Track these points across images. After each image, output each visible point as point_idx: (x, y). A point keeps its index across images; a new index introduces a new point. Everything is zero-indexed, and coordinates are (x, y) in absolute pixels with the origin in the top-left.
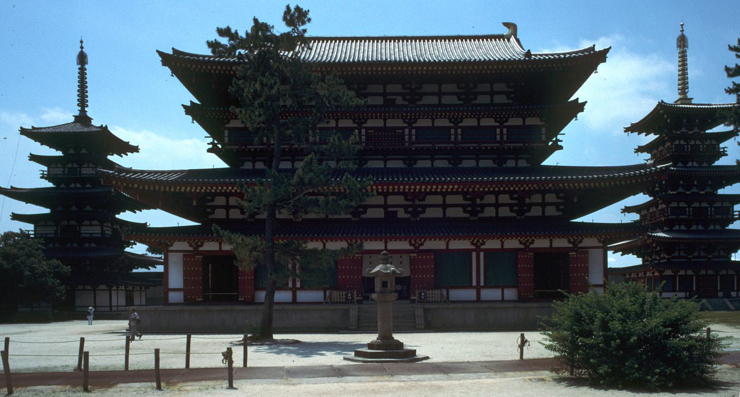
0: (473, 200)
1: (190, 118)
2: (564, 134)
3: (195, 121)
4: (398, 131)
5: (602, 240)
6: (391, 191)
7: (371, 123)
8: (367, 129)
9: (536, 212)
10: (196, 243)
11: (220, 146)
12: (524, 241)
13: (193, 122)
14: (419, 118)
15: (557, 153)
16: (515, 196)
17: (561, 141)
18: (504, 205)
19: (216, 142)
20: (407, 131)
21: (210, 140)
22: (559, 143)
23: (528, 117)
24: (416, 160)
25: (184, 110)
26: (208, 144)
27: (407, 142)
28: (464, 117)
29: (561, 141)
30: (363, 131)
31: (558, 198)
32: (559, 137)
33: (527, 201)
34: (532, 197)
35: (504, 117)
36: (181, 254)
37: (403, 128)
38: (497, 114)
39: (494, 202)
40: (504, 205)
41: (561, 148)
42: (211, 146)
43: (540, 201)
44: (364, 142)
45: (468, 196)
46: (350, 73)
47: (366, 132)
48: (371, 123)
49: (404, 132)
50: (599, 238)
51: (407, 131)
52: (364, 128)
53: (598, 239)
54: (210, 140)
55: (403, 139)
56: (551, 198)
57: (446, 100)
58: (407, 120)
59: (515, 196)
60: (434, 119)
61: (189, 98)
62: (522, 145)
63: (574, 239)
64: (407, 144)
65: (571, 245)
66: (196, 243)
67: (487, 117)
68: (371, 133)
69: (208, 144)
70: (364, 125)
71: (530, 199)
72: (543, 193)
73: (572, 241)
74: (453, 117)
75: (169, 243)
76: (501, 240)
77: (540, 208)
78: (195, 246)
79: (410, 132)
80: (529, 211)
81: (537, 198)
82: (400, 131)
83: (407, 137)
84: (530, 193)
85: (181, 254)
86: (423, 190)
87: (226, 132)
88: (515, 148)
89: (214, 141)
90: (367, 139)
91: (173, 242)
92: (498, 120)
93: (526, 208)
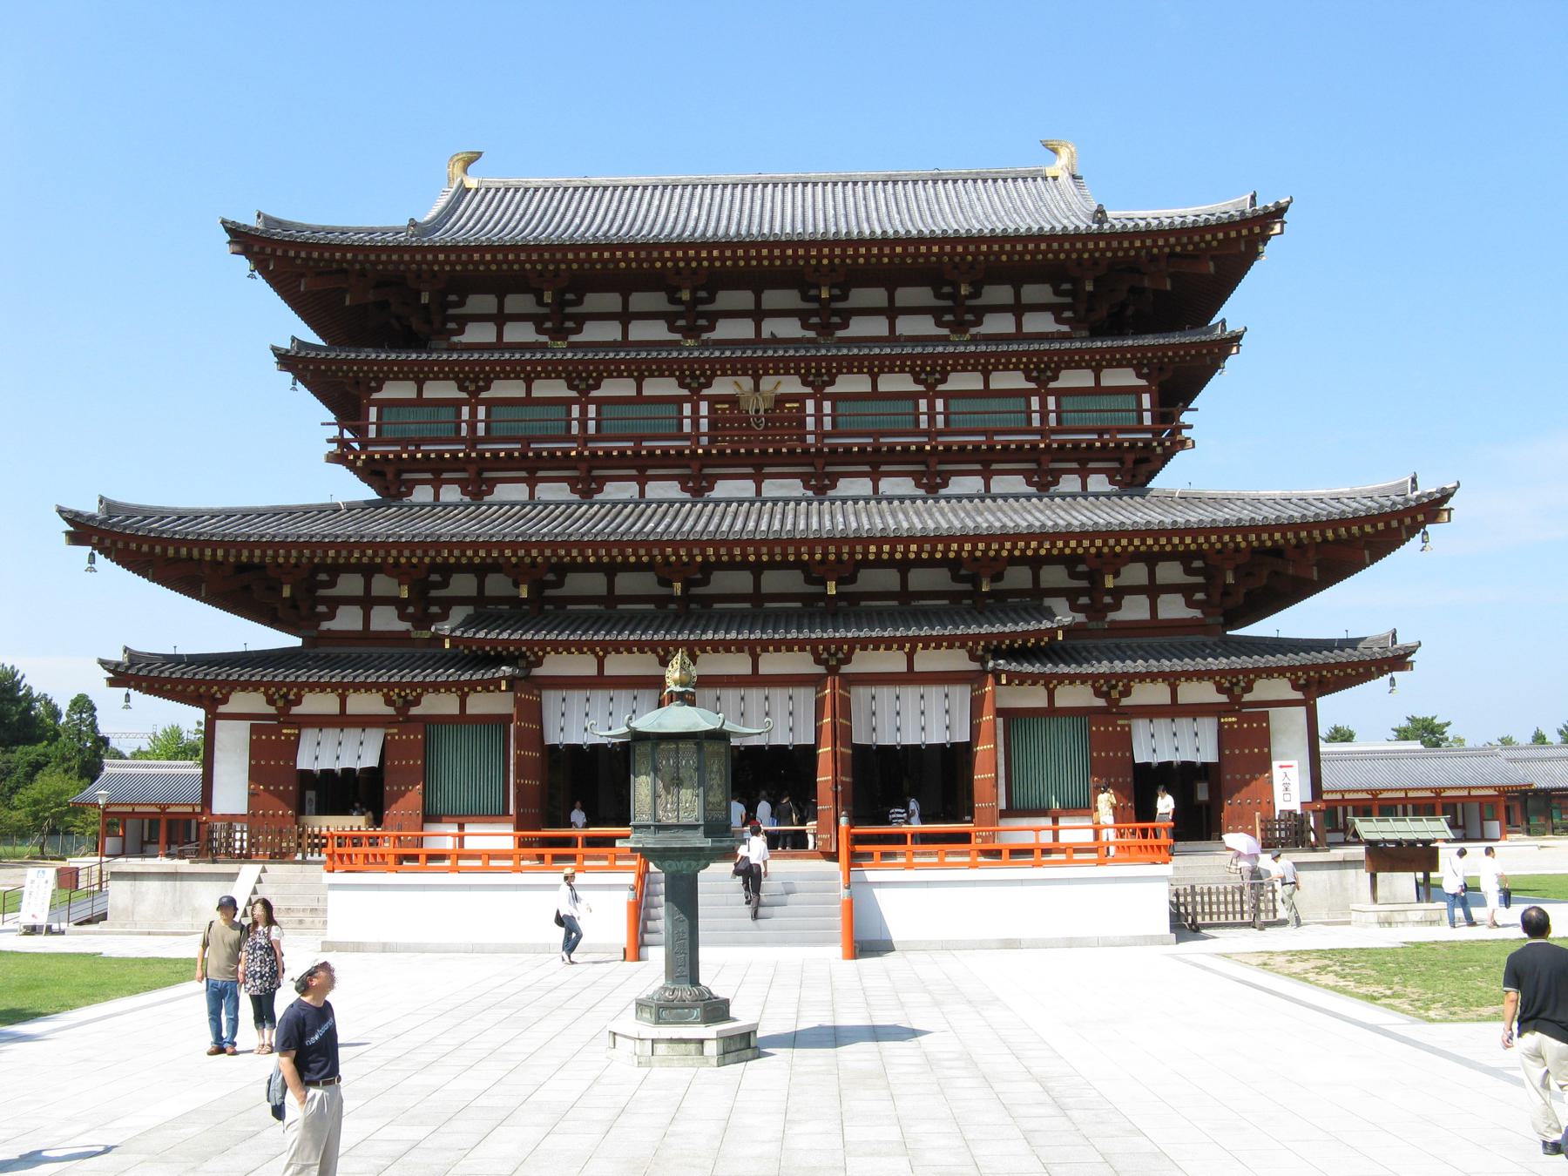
0: (975, 580)
1: (288, 377)
2: (1196, 410)
3: (299, 385)
4: (787, 405)
5: (1302, 681)
6: (765, 558)
7: (722, 386)
8: (713, 400)
9: (1134, 609)
10: (281, 697)
11: (356, 446)
12: (1105, 688)
13: (294, 389)
14: (840, 372)
15: (1180, 457)
16: (1082, 568)
17: (1190, 427)
18: (1056, 592)
19: (347, 435)
20: (810, 406)
21: (334, 431)
22: (1185, 433)
23: (1106, 367)
24: (834, 479)
25: (276, 360)
26: (330, 441)
27: (811, 433)
28: (949, 368)
29: (1190, 427)
30: (704, 408)
31: (1189, 571)
32: (1185, 418)
33: (1109, 582)
35: (1048, 367)
36: (247, 724)
37: (800, 398)
38: (1152, 358)
39: (1029, 585)
40: (1056, 592)
41: (1182, 444)
42: (334, 447)
44: (704, 435)
46: (669, 264)
47: (712, 410)
48: (722, 386)
49: (803, 408)
50: (1293, 677)
51: (810, 406)
52: (705, 398)
53: (1289, 679)
54: (334, 431)
55: (803, 424)
56: (1170, 572)
57: (908, 326)
58: (811, 378)
59: (1082, 568)
60: (877, 375)
61: (292, 328)
62: (1096, 437)
63: (1230, 682)
64: (811, 439)
65: (1223, 698)
66: (281, 697)
67: (1006, 369)
68: (724, 410)
69: (330, 441)
70: (705, 392)
71: (1116, 575)
72: (1151, 559)
73: (1227, 685)
74: (923, 370)
75: (219, 696)
76: (1046, 685)
77: (1143, 600)
78: (280, 703)
79: (819, 408)
80: (1117, 606)
81: (1135, 574)
82: (796, 405)
83: (810, 423)
84: (1115, 562)
85: (245, 725)
86: (846, 557)
87: (373, 411)
88: (1076, 444)
89: (341, 433)
90: (712, 425)
91: (229, 693)
92: (1035, 374)
93: (1108, 600)
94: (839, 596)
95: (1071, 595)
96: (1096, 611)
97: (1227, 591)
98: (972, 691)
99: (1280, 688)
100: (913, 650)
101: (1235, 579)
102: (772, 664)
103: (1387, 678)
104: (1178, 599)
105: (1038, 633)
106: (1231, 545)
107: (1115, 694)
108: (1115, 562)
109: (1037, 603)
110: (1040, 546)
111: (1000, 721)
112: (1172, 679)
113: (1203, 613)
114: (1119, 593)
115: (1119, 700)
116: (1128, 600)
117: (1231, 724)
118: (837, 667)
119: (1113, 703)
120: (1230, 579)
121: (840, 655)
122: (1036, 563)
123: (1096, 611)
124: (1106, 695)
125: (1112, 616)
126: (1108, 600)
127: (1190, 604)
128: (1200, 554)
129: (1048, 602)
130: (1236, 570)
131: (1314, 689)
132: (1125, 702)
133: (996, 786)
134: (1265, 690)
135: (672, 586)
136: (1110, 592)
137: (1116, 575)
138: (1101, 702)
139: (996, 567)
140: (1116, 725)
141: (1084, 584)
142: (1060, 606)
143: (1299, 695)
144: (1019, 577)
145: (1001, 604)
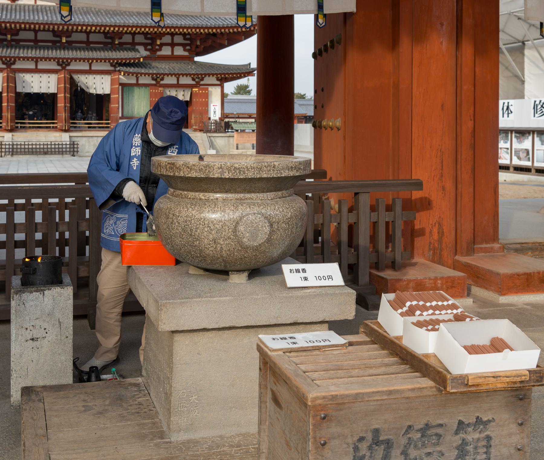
0: (113, 39)
5: (220, 78)
9: (166, 51)
12: (155, 78)
33: (158, 42)
34: (163, 38)
39: (131, 41)
40: (140, 44)
43: (169, 41)
45: (108, 35)
71: (161, 39)
77: (169, 48)
80: (160, 50)
81: (167, 39)
84: (161, 35)
93: (157, 47)
94: (67, 42)
95: (145, 45)
96: (153, 51)
97: (197, 47)
98: (111, 77)
99: (213, 80)
100: (91, 63)
101: (200, 43)
102: (42, 66)
103: (246, 78)
104: (181, 48)
105: (134, 59)
106: (199, 33)
107: (158, 80)
108: (161, 35)
109: (133, 47)
110: (136, 29)
111: (120, 87)
112: (178, 76)
113: (189, 53)
114: (162, 45)
115: (160, 82)
116: (164, 48)
117: (196, 91)
118: (65, 67)
119: (158, 83)
120: (198, 43)
121: (66, 63)
122: (134, 34)
123: (153, 51)
124: (156, 80)
125: (159, 53)
126: (157, 47)
127: (185, 50)
128: (189, 34)
129: (137, 47)
130: (201, 40)
131: (224, 80)
132: (162, 82)
133: (118, 108)
134: (207, 80)
135: (7, 37)
136: (158, 45)
137: (161, 39)
138: (154, 82)
139: (120, 35)
140: (158, 90)
141: (149, 41)
142: (141, 49)
143: (218, 83)
144: (127, 38)
145: (121, 47)
